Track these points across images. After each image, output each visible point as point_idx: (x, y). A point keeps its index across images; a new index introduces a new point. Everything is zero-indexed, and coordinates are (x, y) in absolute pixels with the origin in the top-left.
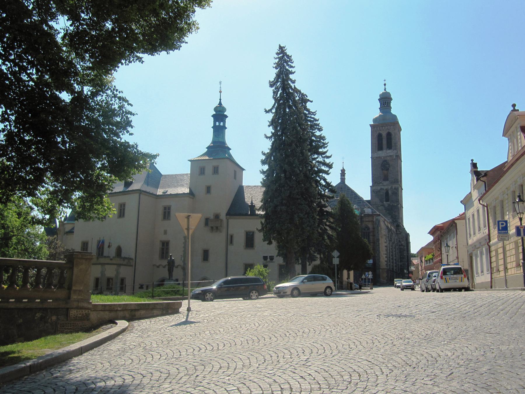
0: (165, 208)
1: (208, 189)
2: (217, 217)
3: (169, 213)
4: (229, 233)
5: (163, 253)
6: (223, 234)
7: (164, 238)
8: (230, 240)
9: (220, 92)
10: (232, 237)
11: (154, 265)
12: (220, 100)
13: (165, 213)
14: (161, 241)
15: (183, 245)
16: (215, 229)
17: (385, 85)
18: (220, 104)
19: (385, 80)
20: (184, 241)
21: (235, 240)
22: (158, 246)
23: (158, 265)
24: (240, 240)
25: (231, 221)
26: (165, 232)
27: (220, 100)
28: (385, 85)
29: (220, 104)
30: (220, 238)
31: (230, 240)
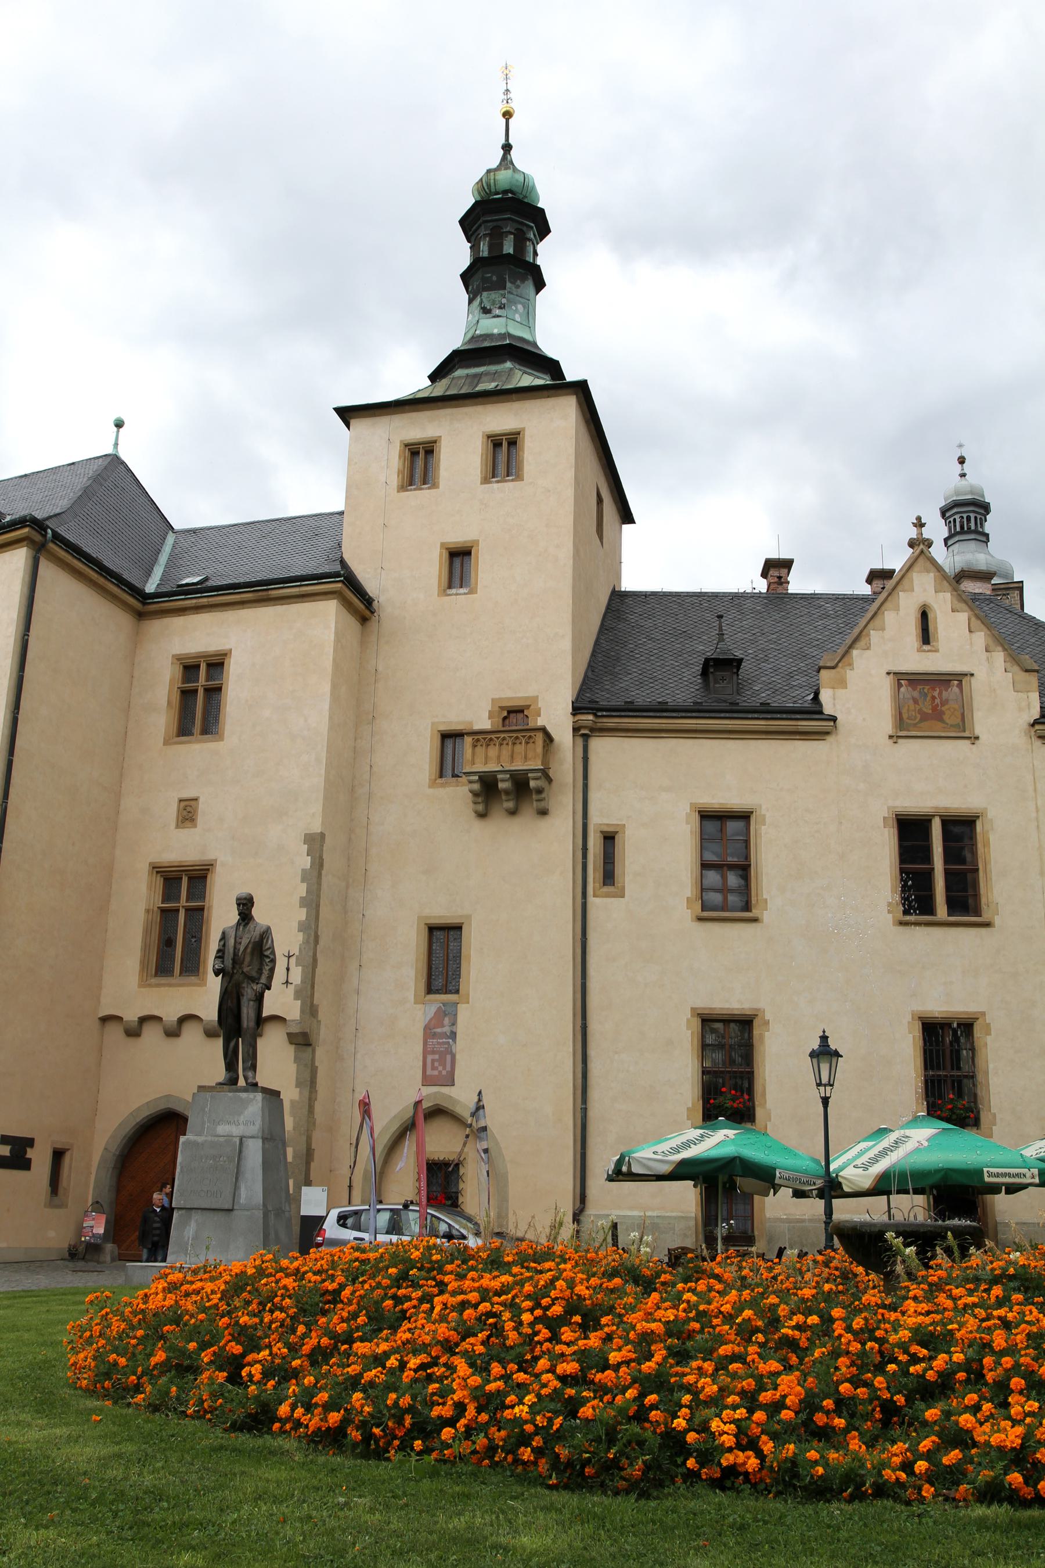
0: (189, 668)
1: (459, 559)
2: (515, 719)
3: (214, 692)
4: (598, 819)
5: (167, 942)
6: (561, 825)
7: (182, 848)
8: (603, 860)
9: (507, 115)
10: (609, 839)
11: (105, 1020)
12: (507, 148)
13: (187, 695)
14: (157, 869)
15: (302, 890)
16: (509, 796)
17: (962, 461)
18: (506, 160)
19: (960, 446)
20: (306, 862)
21: (632, 860)
22: (136, 901)
23: (131, 1015)
24: (664, 858)
25: (600, 746)
26: (188, 813)
27: (507, 148)
28: (962, 461)
29: (506, 160)
30: (544, 846)
31: (603, 860)
